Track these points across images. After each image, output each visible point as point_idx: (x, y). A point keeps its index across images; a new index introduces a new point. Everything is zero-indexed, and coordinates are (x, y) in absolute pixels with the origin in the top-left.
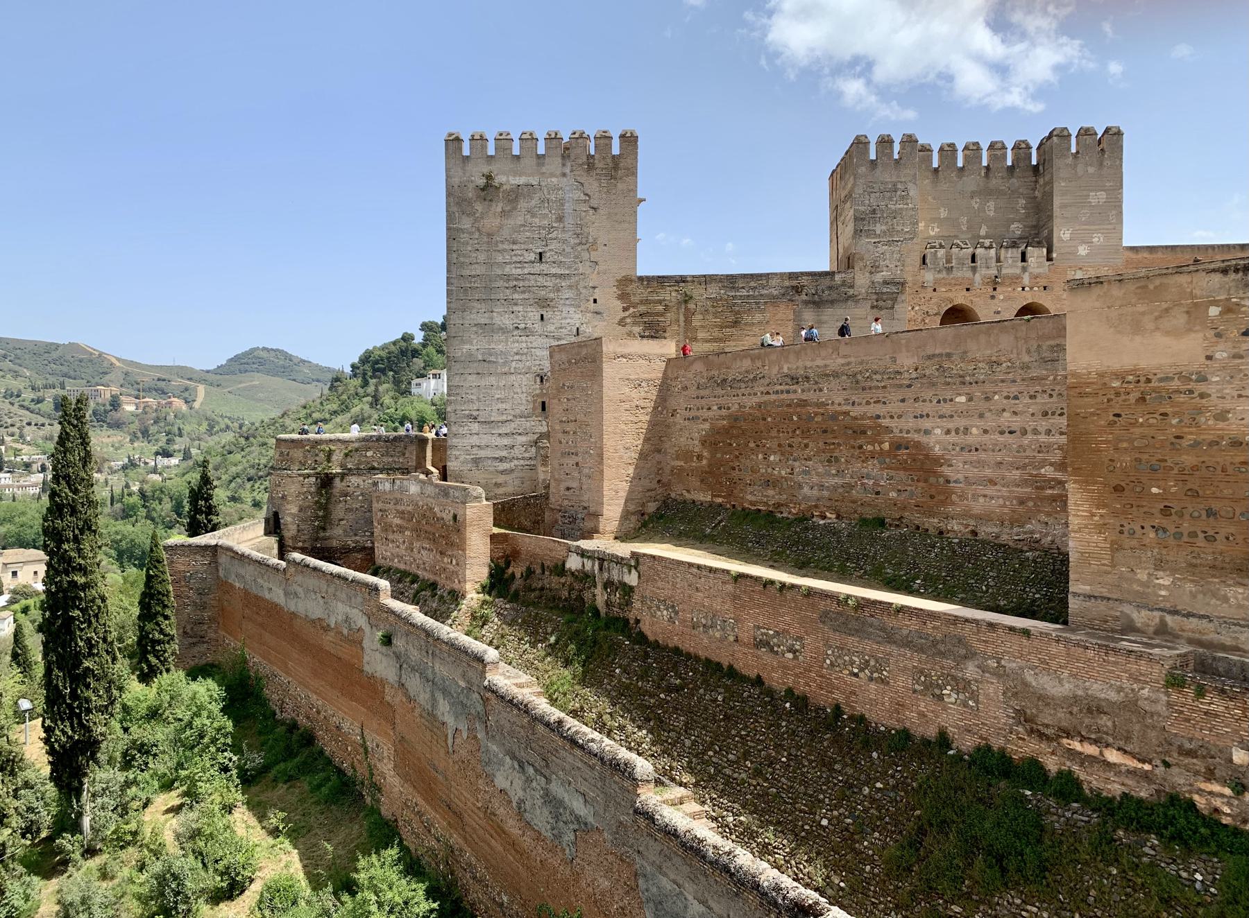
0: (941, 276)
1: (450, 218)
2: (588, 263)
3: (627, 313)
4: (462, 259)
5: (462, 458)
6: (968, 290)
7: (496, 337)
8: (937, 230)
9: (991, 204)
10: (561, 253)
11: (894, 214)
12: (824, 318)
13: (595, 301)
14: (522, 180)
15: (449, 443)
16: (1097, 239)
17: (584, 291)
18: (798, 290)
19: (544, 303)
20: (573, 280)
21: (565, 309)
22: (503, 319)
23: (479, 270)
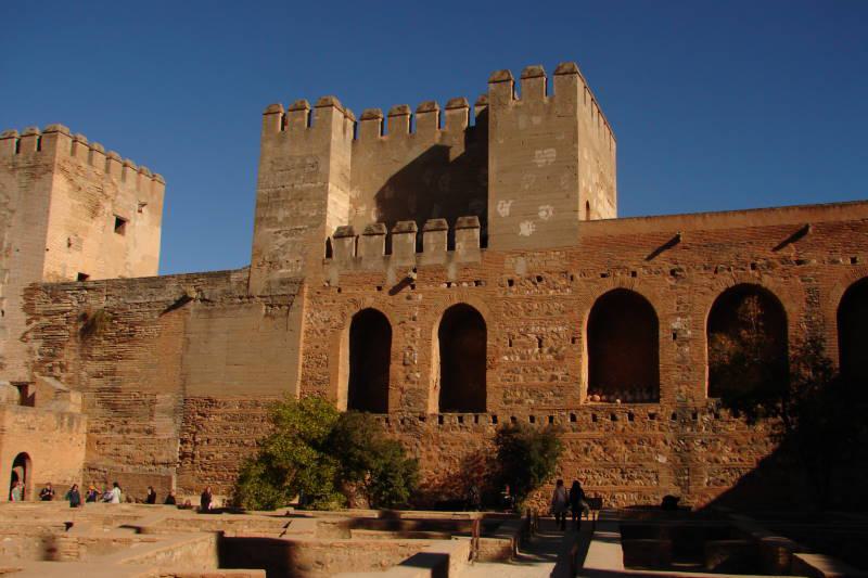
16: (545, 213)
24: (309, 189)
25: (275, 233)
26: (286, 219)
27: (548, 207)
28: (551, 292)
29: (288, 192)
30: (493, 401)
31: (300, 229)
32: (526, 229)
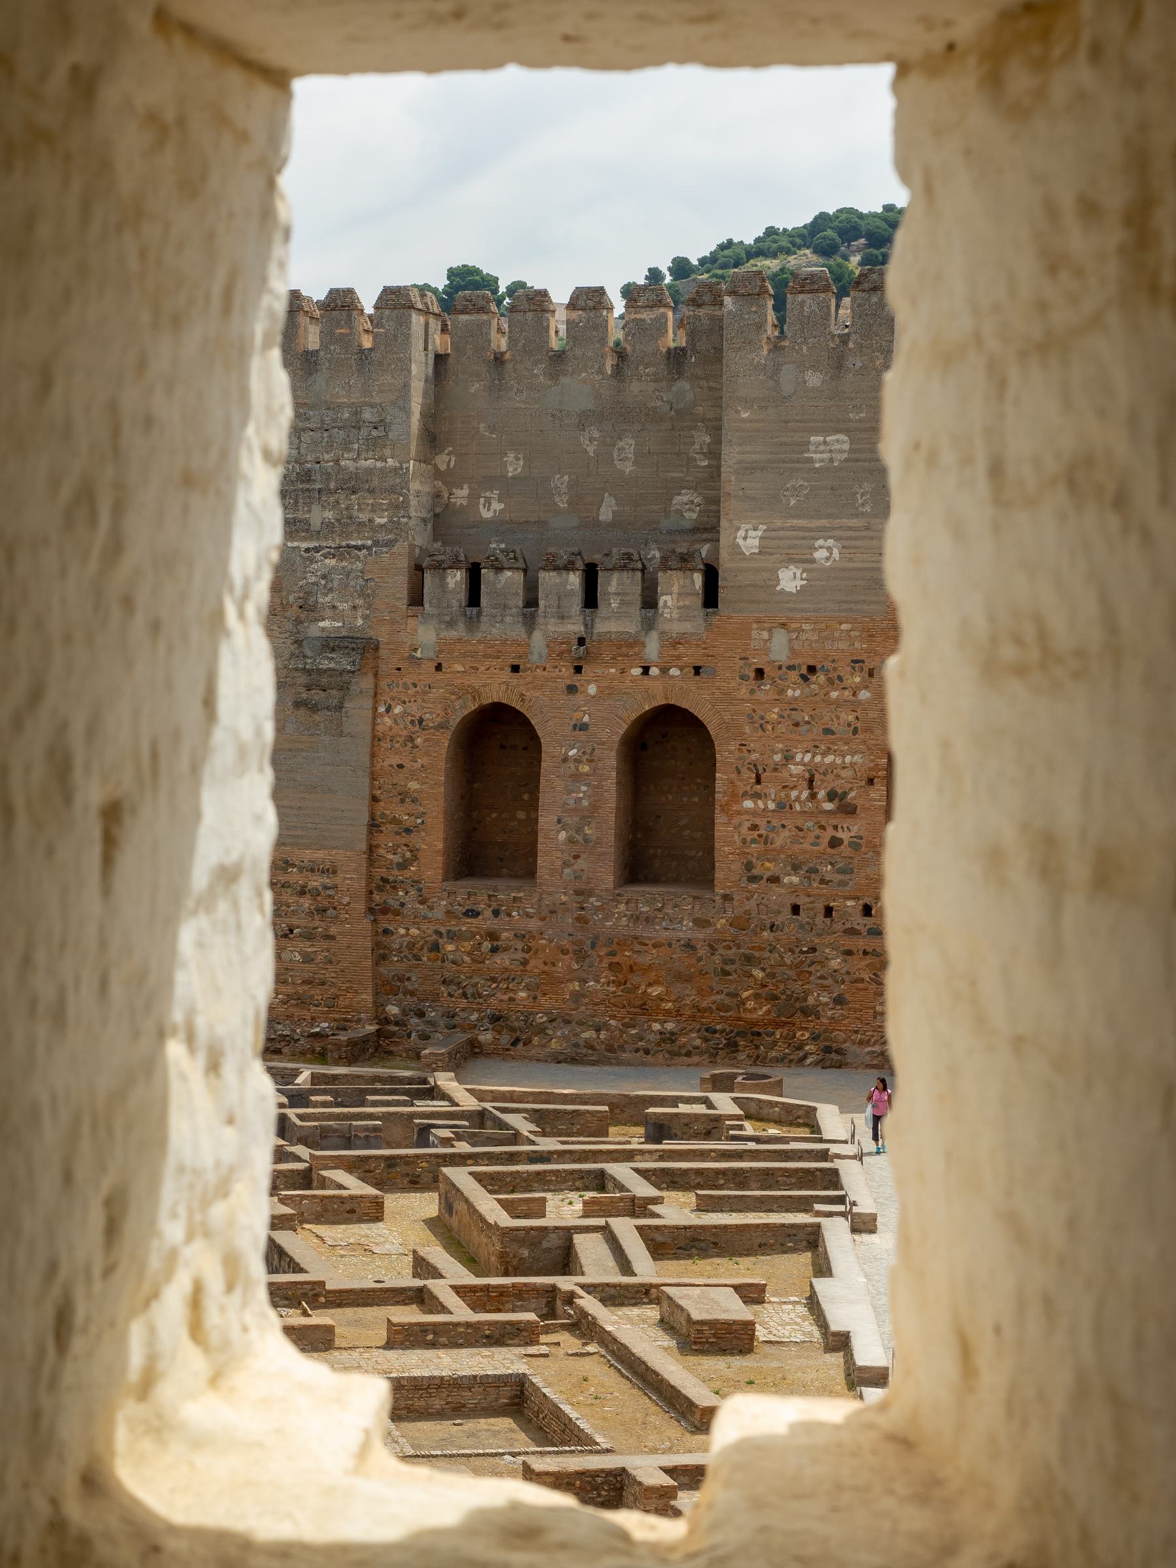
0: (453, 634)
6: (515, 669)
8: (497, 506)
11: (353, 484)
16: (825, 552)
24: (370, 471)
25: (307, 550)
26: (328, 526)
27: (831, 542)
28: (834, 695)
29: (327, 476)
30: (727, 870)
32: (790, 580)
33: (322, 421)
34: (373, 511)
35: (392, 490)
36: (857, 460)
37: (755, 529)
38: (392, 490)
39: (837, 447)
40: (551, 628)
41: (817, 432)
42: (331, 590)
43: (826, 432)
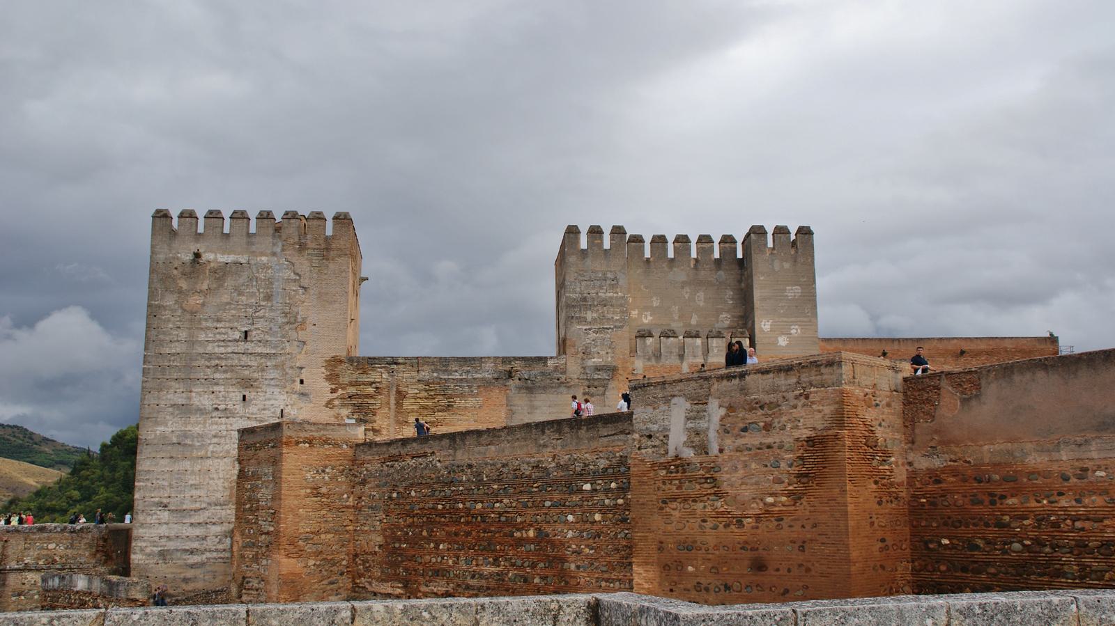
1: (152, 294)
2: (296, 343)
3: (335, 395)
4: (162, 337)
5: (148, 550)
7: (193, 419)
8: (650, 318)
9: (701, 295)
10: (269, 331)
12: (537, 403)
13: (302, 382)
14: (230, 258)
15: (135, 533)
17: (290, 371)
18: (510, 375)
19: (247, 383)
20: (279, 359)
21: (269, 390)
22: (202, 399)
23: (177, 348)
24: (611, 298)
25: (586, 330)
26: (594, 320)
27: (797, 327)
31: (606, 328)
33: (590, 277)
34: (613, 314)
35: (621, 305)
36: (804, 296)
37: (768, 322)
38: (621, 305)
39: (796, 291)
40: (691, 360)
41: (788, 285)
42: (596, 346)
43: (793, 285)
